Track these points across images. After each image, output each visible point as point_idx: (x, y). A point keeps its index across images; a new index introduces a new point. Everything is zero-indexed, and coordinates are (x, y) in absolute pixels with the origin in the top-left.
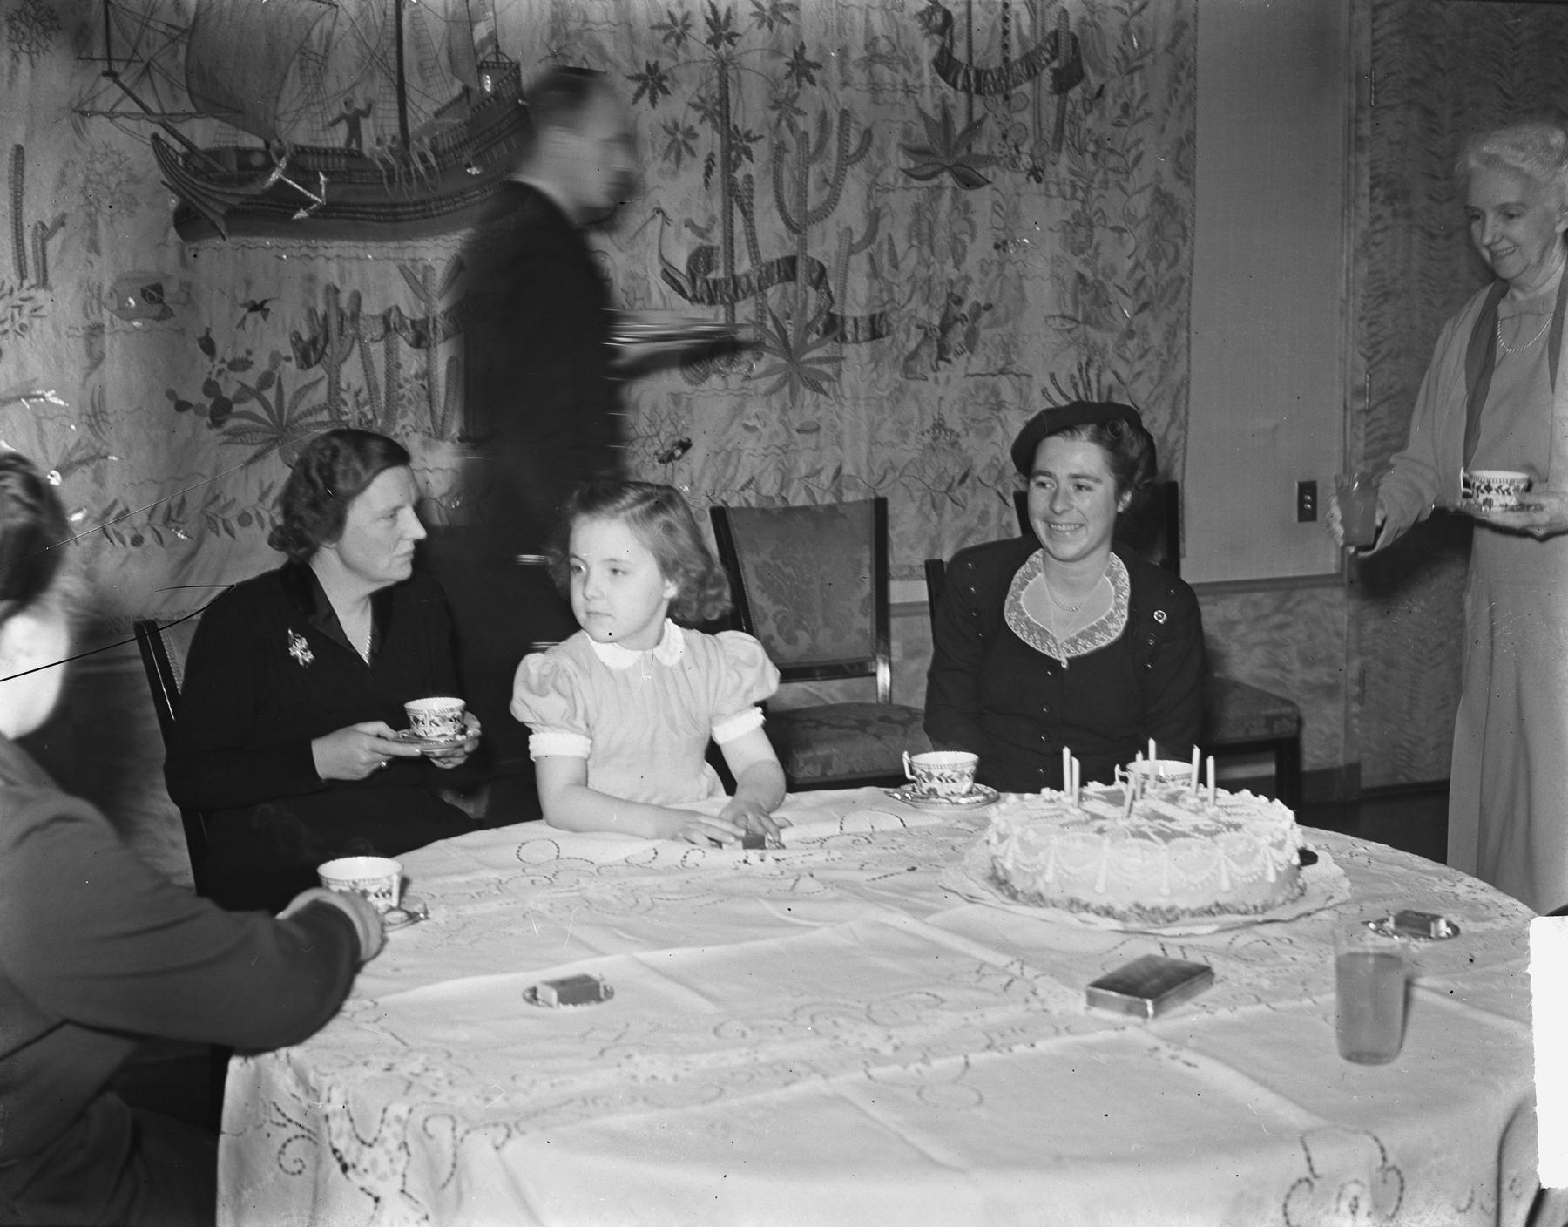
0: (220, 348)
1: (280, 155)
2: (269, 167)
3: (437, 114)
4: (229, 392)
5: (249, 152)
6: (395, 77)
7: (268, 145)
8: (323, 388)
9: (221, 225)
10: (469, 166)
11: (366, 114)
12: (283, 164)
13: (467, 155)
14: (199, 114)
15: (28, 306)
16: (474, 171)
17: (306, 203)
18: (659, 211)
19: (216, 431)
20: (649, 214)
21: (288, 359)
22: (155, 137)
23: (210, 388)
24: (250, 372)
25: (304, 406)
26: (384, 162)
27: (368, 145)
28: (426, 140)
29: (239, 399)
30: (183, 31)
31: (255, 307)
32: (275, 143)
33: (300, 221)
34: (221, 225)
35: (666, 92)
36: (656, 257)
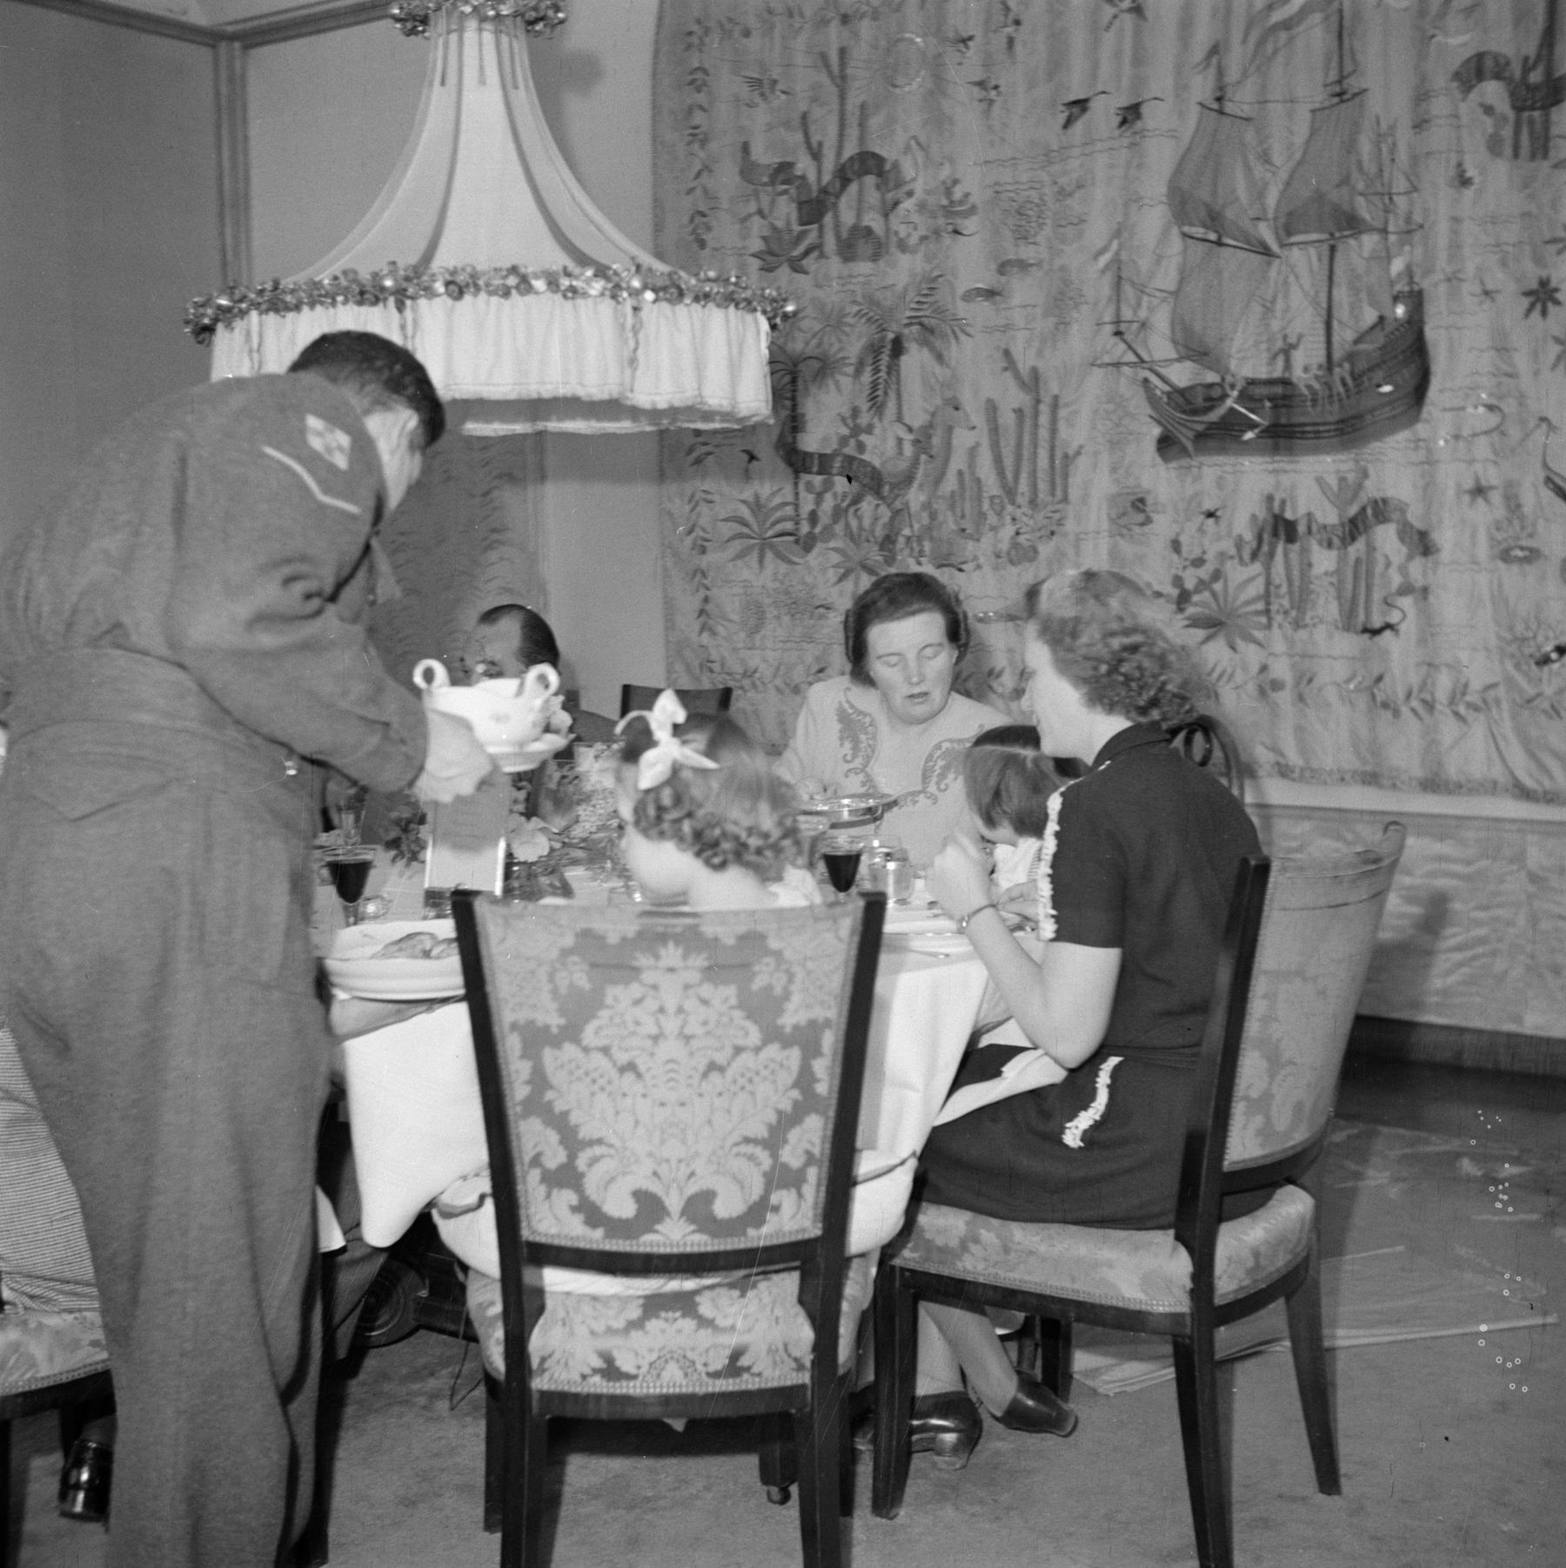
0: (1185, 549)
1: (1233, 386)
2: (1224, 396)
3: (1357, 342)
4: (1190, 584)
5: (1211, 386)
6: (1324, 313)
7: (1223, 379)
8: (1261, 581)
9: (1189, 445)
10: (1379, 386)
11: (1293, 347)
12: (1235, 393)
13: (1379, 375)
14: (1180, 359)
15: (1057, 516)
16: (1387, 389)
17: (1252, 425)
18: (1543, 419)
19: (1180, 616)
20: (1532, 422)
21: (1232, 557)
22: (1146, 380)
23: (1177, 581)
24: (1204, 568)
25: (1243, 597)
26: (1309, 387)
27: (1298, 375)
28: (1347, 366)
29: (1197, 591)
30: (1171, 293)
31: (1210, 515)
32: (1229, 379)
33: (1247, 442)
34: (1189, 445)
35: (1557, 303)
36: (1539, 465)
